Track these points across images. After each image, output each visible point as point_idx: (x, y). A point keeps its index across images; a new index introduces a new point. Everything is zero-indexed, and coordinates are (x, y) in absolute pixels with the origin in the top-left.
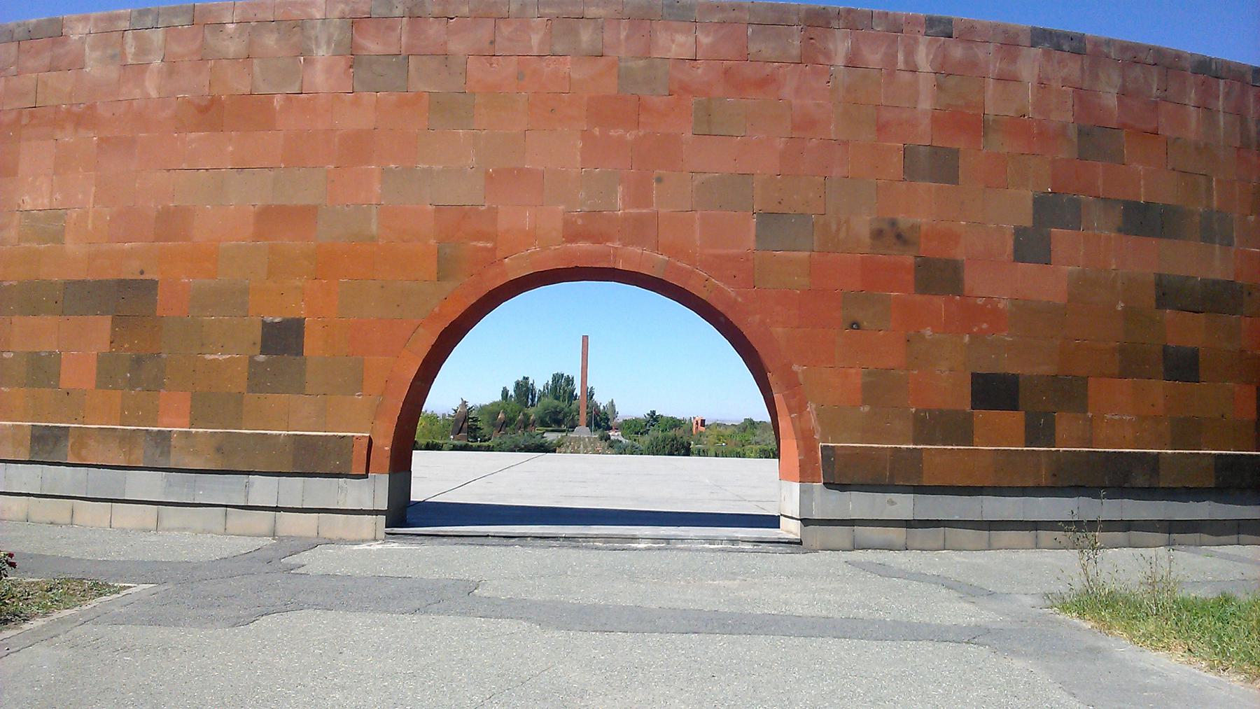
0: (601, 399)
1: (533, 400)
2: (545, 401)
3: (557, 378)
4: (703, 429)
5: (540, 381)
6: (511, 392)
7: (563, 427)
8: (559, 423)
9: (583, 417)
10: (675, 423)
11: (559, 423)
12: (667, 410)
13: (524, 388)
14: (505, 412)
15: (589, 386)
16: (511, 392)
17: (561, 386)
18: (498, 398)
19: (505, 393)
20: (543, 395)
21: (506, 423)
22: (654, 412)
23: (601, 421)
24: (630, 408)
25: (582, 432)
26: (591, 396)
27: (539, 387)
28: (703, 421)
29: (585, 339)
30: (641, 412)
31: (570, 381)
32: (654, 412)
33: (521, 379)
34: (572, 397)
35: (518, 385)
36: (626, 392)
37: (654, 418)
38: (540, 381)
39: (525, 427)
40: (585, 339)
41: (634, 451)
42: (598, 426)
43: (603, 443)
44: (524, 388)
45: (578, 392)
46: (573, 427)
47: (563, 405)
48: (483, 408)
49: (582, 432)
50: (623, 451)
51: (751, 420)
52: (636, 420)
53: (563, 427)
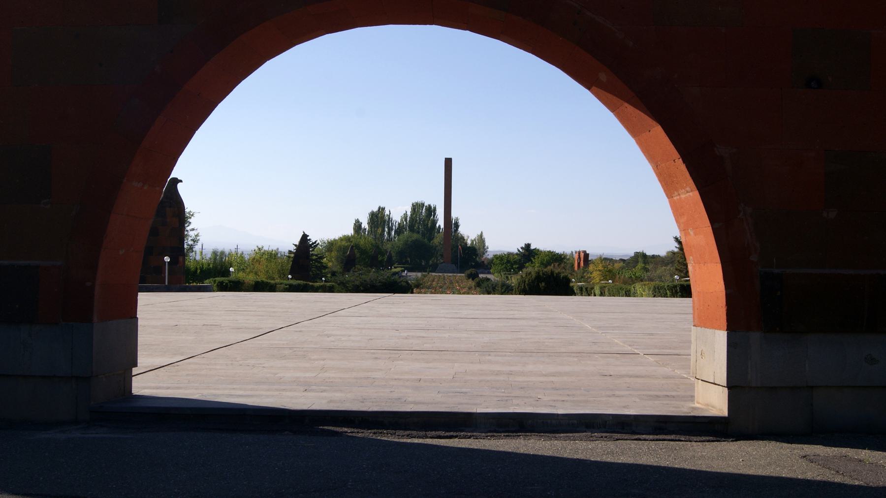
0: (468, 232)
1: (389, 233)
3: (417, 207)
6: (365, 225)
10: (557, 258)
13: (378, 218)
15: (454, 215)
16: (365, 225)
17: (421, 216)
18: (350, 231)
19: (358, 226)
22: (528, 246)
24: (502, 241)
26: (457, 226)
29: (448, 162)
31: (431, 211)
33: (376, 210)
36: (494, 223)
38: (398, 212)
40: (448, 162)
41: (506, 290)
43: (471, 283)
44: (378, 218)
45: (441, 223)
50: (490, 289)
51: (644, 256)
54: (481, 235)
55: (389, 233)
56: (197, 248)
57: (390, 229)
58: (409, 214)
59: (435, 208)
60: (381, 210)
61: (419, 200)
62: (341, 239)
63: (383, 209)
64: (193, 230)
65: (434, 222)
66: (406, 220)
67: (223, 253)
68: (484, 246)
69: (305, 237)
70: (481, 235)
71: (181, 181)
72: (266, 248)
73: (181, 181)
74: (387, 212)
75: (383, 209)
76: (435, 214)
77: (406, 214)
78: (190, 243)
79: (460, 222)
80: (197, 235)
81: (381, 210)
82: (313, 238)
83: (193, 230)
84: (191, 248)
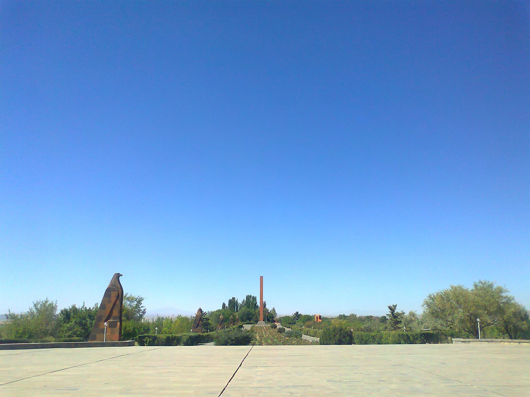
0: (269, 307)
1: (237, 309)
2: (243, 309)
3: (248, 297)
4: (321, 320)
5: (241, 299)
6: (227, 305)
7: (252, 322)
8: (250, 319)
9: (261, 317)
11: (250, 319)
12: (303, 312)
13: (233, 302)
14: (223, 315)
16: (227, 305)
17: (250, 301)
18: (221, 308)
19: (224, 305)
20: (242, 306)
21: (224, 320)
23: (270, 317)
25: (261, 324)
27: (240, 302)
28: (320, 316)
29: (262, 278)
30: (291, 313)
31: (254, 299)
32: (297, 313)
34: (256, 306)
35: (230, 301)
37: (297, 315)
38: (241, 299)
39: (234, 322)
40: (262, 278)
42: (269, 320)
44: (233, 302)
45: (258, 304)
46: (257, 322)
47: (252, 311)
48: (212, 314)
49: (261, 324)
52: (288, 317)
53: (252, 322)
55: (237, 309)
56: (144, 316)
60: (234, 298)
61: (249, 294)
62: (217, 311)
64: (142, 307)
67: (163, 318)
69: (200, 310)
71: (122, 275)
72: (183, 315)
73: (122, 275)
77: (244, 300)
78: (141, 314)
80: (145, 310)
81: (234, 298)
82: (204, 310)
83: (142, 307)
84: (141, 316)
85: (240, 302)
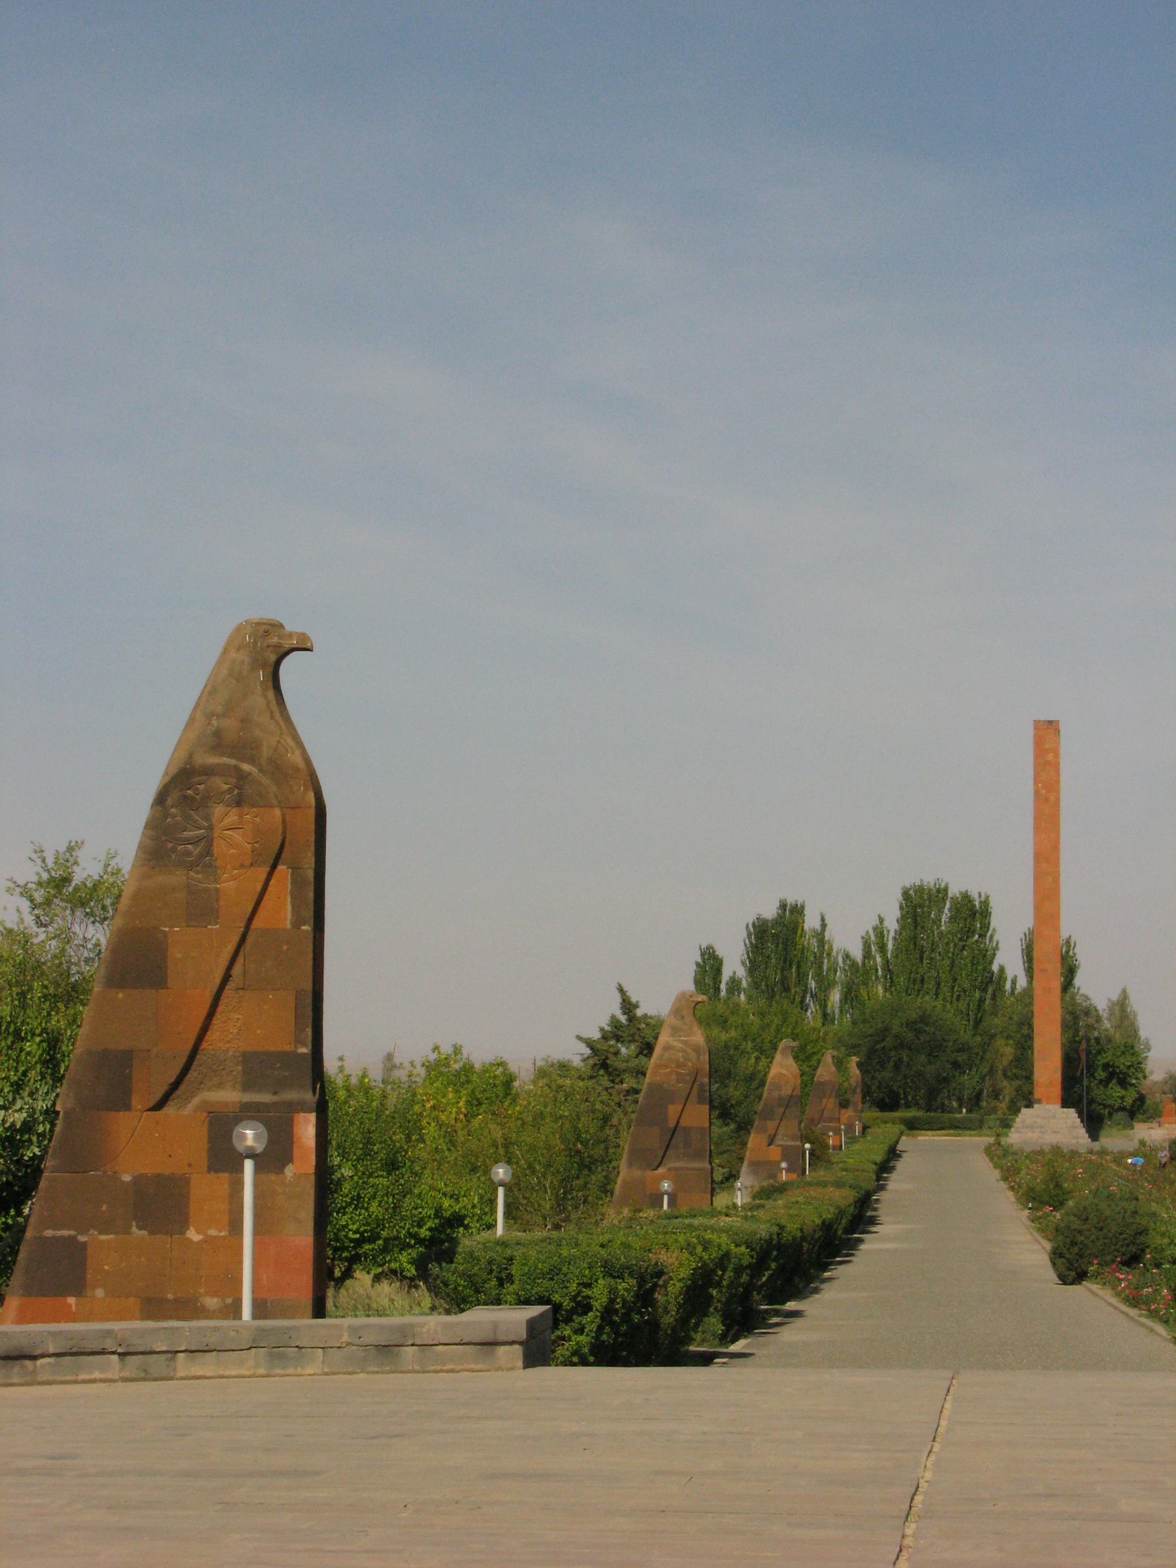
3: (919, 905)
16: (734, 965)
19: (710, 964)
20: (859, 974)
27: (847, 938)
29: (1046, 733)
31: (973, 915)
33: (770, 912)
38: (852, 917)
40: (1046, 733)
44: (781, 943)
45: (1009, 960)
47: (947, 1013)
54: (1124, 996)
57: (825, 986)
58: (892, 925)
59: (985, 904)
60: (791, 914)
61: (929, 878)
63: (798, 910)
65: (985, 956)
66: (882, 948)
68: (1135, 1034)
70: (1124, 996)
74: (811, 922)
75: (798, 910)
76: (986, 926)
77: (880, 932)
79: (1082, 955)
81: (791, 914)
85: (847, 938)
